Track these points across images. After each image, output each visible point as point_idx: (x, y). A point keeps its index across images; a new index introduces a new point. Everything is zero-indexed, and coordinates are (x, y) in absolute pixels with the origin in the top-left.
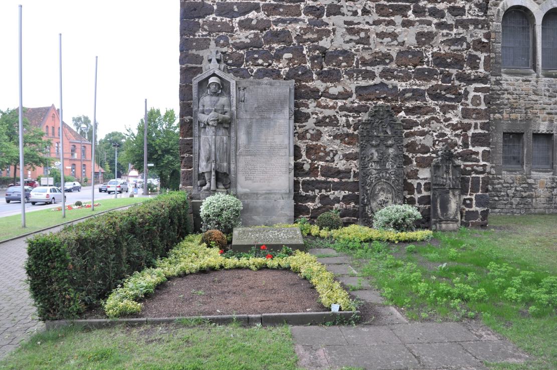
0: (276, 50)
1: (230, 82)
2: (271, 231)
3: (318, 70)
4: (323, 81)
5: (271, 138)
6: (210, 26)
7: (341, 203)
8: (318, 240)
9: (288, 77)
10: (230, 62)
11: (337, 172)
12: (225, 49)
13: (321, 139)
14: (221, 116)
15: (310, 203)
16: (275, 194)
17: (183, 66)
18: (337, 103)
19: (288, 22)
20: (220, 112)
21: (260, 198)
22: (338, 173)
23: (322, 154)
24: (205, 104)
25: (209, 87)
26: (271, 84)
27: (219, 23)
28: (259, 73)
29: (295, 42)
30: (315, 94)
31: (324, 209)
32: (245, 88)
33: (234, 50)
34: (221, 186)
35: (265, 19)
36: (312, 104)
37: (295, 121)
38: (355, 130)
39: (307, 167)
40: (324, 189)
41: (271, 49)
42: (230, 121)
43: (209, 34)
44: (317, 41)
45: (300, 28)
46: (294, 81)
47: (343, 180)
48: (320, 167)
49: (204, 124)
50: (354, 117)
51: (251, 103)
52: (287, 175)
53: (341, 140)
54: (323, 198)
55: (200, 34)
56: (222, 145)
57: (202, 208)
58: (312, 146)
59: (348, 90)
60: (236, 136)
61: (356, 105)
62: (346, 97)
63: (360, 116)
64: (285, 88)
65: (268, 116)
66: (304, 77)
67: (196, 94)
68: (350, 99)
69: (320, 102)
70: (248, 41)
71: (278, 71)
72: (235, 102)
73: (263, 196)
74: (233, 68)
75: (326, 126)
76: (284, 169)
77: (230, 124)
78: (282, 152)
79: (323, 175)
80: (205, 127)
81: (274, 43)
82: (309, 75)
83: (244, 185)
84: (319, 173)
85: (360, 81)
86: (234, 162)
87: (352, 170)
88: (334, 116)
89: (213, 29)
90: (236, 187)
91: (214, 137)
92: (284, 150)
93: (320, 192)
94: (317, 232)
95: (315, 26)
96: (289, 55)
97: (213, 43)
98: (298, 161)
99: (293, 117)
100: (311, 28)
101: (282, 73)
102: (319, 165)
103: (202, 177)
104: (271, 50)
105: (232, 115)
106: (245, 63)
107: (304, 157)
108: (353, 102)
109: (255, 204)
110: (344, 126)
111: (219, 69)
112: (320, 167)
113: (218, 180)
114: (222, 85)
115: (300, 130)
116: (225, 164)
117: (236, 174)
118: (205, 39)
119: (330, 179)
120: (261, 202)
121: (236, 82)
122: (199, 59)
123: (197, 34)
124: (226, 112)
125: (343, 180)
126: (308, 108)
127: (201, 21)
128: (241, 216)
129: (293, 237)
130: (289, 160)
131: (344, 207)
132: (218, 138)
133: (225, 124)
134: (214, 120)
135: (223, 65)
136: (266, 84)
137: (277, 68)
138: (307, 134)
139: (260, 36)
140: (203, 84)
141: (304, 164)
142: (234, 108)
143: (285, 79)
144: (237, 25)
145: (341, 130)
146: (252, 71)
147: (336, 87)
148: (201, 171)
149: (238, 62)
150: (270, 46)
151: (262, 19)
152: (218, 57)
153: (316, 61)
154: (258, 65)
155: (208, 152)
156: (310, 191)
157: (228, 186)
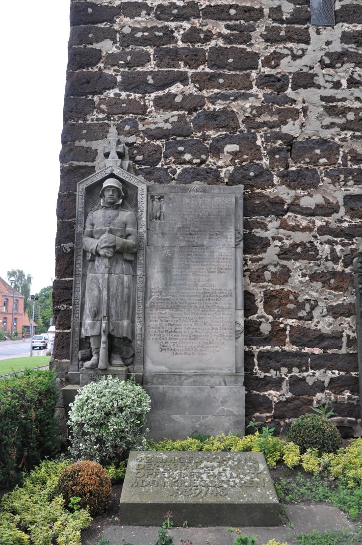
0: (213, 139)
1: (137, 188)
2: (205, 463)
3: (282, 169)
4: (289, 186)
5: (204, 278)
6: (109, 105)
7: (327, 391)
8: (300, 478)
9: (233, 181)
10: (139, 158)
11: (317, 337)
12: (132, 139)
13: (290, 280)
14: (120, 241)
15: (272, 392)
16: (212, 375)
17: (66, 165)
18: (314, 222)
19: (232, 98)
20: (119, 234)
21: (186, 382)
22: (319, 339)
23: (291, 306)
24: (95, 222)
25: (102, 196)
26: (204, 191)
27: (123, 102)
28: (187, 175)
29: (242, 127)
30: (277, 208)
31: (297, 402)
32: (162, 197)
33: (146, 140)
34: (117, 361)
35: (196, 93)
36: (273, 224)
37: (246, 251)
38: (346, 266)
39: (265, 328)
40: (297, 367)
41: (205, 138)
42: (135, 250)
43: (108, 118)
44: (279, 126)
45: (251, 106)
46: (242, 186)
47: (330, 352)
48: (288, 328)
49: (92, 254)
50: (343, 245)
51: (172, 219)
52: (233, 342)
53: (324, 283)
54: (295, 383)
55: (95, 117)
56: (120, 290)
57: (74, 406)
58: (274, 293)
59: (331, 200)
60: (146, 275)
61: (346, 224)
62: (329, 211)
63: (353, 243)
64: (229, 198)
65: (199, 242)
66: (259, 180)
67: (82, 206)
68: (336, 216)
69: (285, 220)
70: (169, 126)
71: (216, 171)
72: (144, 219)
73: (191, 380)
74: (143, 167)
75: (296, 260)
76: (227, 333)
77: (135, 254)
78: (224, 303)
79: (293, 343)
80: (93, 260)
81: (209, 129)
82: (267, 177)
83: (156, 361)
84: (288, 340)
85: (350, 186)
86: (142, 319)
87: (344, 334)
88: (310, 242)
89: (114, 110)
90: (143, 362)
91: (106, 276)
92: (227, 299)
93: (290, 371)
94: (297, 458)
95: (274, 103)
96: (235, 148)
97: (113, 130)
98: (251, 318)
99: (242, 244)
100: (268, 107)
101: (222, 175)
102: (286, 325)
103: (87, 345)
104: (204, 140)
105: (139, 239)
106: (162, 160)
107: (261, 311)
108: (340, 221)
109: (176, 392)
110: (327, 260)
111: (121, 167)
112: (288, 328)
113: (112, 350)
114: (126, 193)
115: (253, 266)
116: (125, 323)
117: (144, 340)
118: (102, 125)
119: (306, 350)
120: (186, 390)
121: (148, 187)
122: (91, 155)
123: (89, 117)
124: (129, 235)
125: (330, 352)
126: (267, 230)
127: (96, 98)
128: (146, 428)
129: (251, 482)
130: (236, 316)
131: (333, 398)
132: (114, 277)
133: (127, 254)
134: (107, 247)
135: (127, 163)
136: (197, 191)
137: (215, 167)
138: (266, 272)
139: (188, 119)
140: (94, 191)
141: (261, 323)
142: (142, 229)
143: (227, 184)
144: (152, 103)
145: (322, 267)
146: (174, 172)
147: (311, 196)
148: (84, 334)
149: (152, 158)
150: (204, 134)
151: (191, 94)
152: (120, 150)
153: (277, 156)
154: (185, 162)
155: (96, 302)
156: (272, 371)
157: (129, 361)
